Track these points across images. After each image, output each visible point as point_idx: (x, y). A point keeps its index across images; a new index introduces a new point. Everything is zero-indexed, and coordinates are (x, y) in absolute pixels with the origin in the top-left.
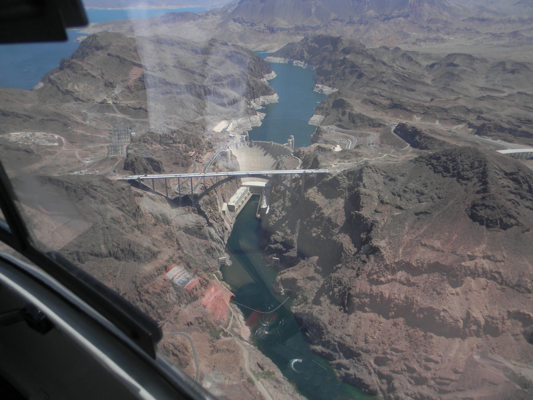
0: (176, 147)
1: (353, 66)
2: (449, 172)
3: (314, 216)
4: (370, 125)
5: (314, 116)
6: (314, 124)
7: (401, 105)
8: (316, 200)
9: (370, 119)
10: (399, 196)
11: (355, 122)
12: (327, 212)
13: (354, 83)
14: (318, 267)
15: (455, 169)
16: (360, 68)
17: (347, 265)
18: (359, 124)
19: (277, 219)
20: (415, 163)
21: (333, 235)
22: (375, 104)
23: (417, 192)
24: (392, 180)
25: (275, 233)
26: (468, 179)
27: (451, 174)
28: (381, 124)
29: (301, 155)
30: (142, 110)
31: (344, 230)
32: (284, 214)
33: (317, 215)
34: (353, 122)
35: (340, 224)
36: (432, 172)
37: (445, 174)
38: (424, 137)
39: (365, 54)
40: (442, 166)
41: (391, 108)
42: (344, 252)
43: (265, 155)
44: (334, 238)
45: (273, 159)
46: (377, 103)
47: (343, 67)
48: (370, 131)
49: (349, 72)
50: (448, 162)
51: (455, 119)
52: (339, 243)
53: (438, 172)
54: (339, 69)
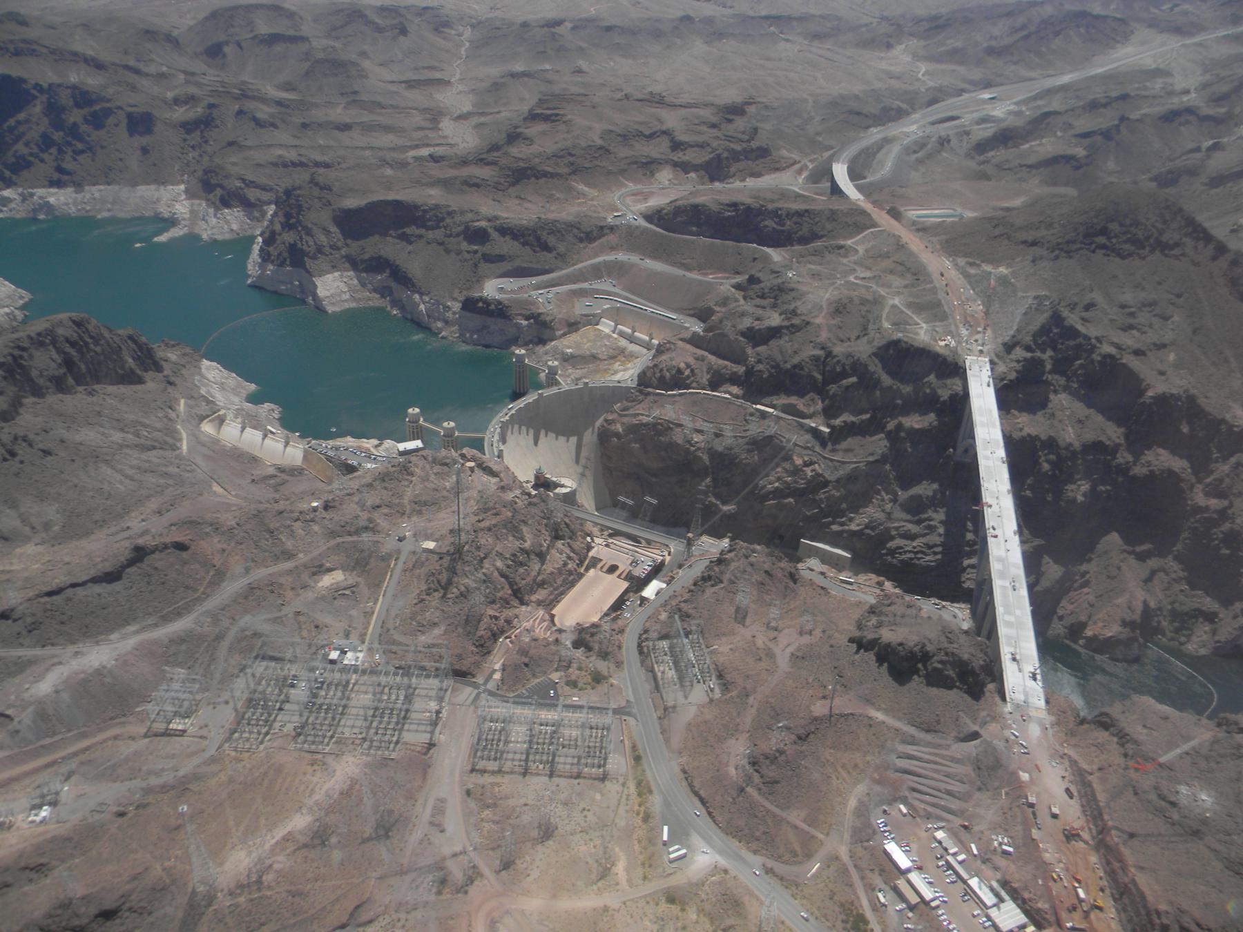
0: (560, 571)
1: (83, 98)
2: (1144, 248)
3: (1046, 466)
4: (581, 240)
5: (318, 281)
6: (347, 306)
7: (532, 168)
8: (1027, 431)
9: (570, 226)
10: (1131, 327)
11: (550, 245)
12: (1069, 435)
13: (145, 151)
14: (1138, 549)
15: (1147, 238)
16: (109, 100)
17: (1235, 491)
18: (561, 248)
19: (935, 539)
20: (1071, 257)
21: (1128, 469)
22: (477, 186)
23: (1144, 305)
24: (1087, 308)
25: (964, 570)
26: (1177, 245)
27: (1148, 248)
28: (602, 228)
29: (688, 377)
30: (157, 560)
31: (1138, 442)
32: (938, 516)
33: (1052, 457)
34: (546, 248)
35: (1117, 441)
36: (1117, 259)
37: (1141, 252)
38: (787, 215)
39: (45, 51)
40: (1126, 242)
41: (513, 184)
42: (1183, 480)
43: (536, 443)
44: (1137, 470)
45: (562, 439)
46: (478, 181)
47: (37, 109)
48: (596, 256)
49: (86, 121)
50: (1133, 230)
51: (635, 163)
52: (1163, 471)
53: (1130, 255)
54: (27, 121)
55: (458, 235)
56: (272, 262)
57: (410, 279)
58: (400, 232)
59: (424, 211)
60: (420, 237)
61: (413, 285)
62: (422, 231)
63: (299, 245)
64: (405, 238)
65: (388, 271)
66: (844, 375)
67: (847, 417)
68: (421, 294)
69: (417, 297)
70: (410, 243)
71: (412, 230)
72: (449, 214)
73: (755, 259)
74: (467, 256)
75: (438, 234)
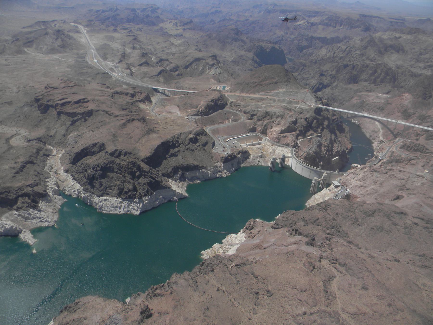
55: (189, 143)
56: (145, 195)
57: (198, 166)
58: (169, 154)
59: (172, 141)
60: (179, 151)
61: (200, 167)
62: (176, 150)
63: (153, 181)
64: (173, 155)
65: (180, 170)
66: (313, 121)
67: (319, 130)
68: (205, 168)
69: (204, 170)
70: (177, 156)
71: (172, 151)
72: (178, 138)
73: (225, 114)
74: (199, 148)
75: (182, 148)
